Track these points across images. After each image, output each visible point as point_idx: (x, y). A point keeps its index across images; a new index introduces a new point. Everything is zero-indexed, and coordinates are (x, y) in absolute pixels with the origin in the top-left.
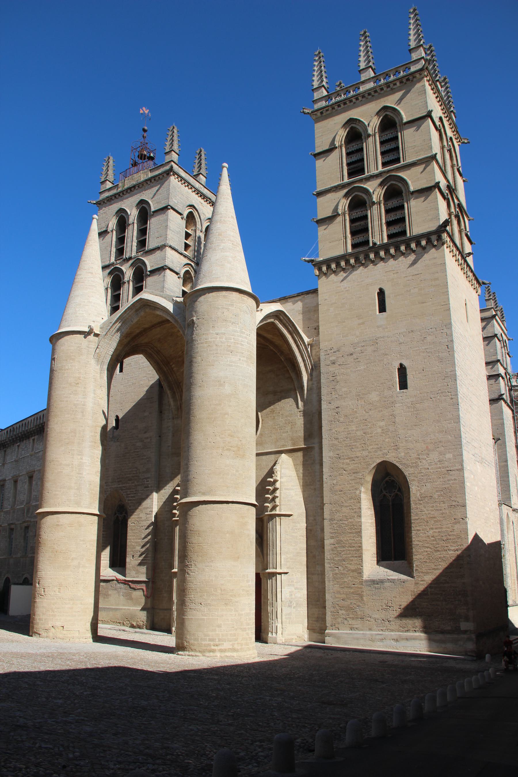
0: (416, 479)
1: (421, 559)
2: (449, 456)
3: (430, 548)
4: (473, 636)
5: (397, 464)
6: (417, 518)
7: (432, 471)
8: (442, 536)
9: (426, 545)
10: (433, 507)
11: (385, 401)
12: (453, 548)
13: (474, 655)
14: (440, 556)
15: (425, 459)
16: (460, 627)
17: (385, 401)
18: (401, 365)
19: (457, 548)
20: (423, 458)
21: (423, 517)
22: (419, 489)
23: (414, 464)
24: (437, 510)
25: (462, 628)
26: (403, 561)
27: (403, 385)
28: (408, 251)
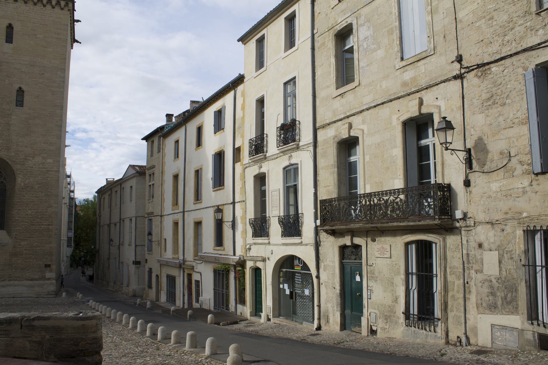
0: (22, 173)
1: (20, 230)
2: (49, 161)
3: (28, 223)
4: (54, 281)
5: (8, 161)
6: (19, 201)
7: (35, 169)
8: (38, 215)
9: (25, 221)
10: (32, 194)
11: (3, 112)
12: (45, 224)
13: (54, 294)
14: (35, 228)
15: (31, 160)
16: (45, 276)
17: (3, 112)
18: (20, 88)
19: (48, 223)
20: (29, 159)
21: (24, 201)
22: (23, 180)
23: (22, 163)
24: (36, 197)
25: (47, 277)
26: (3, 231)
27: (20, 103)
28: (40, 4)
